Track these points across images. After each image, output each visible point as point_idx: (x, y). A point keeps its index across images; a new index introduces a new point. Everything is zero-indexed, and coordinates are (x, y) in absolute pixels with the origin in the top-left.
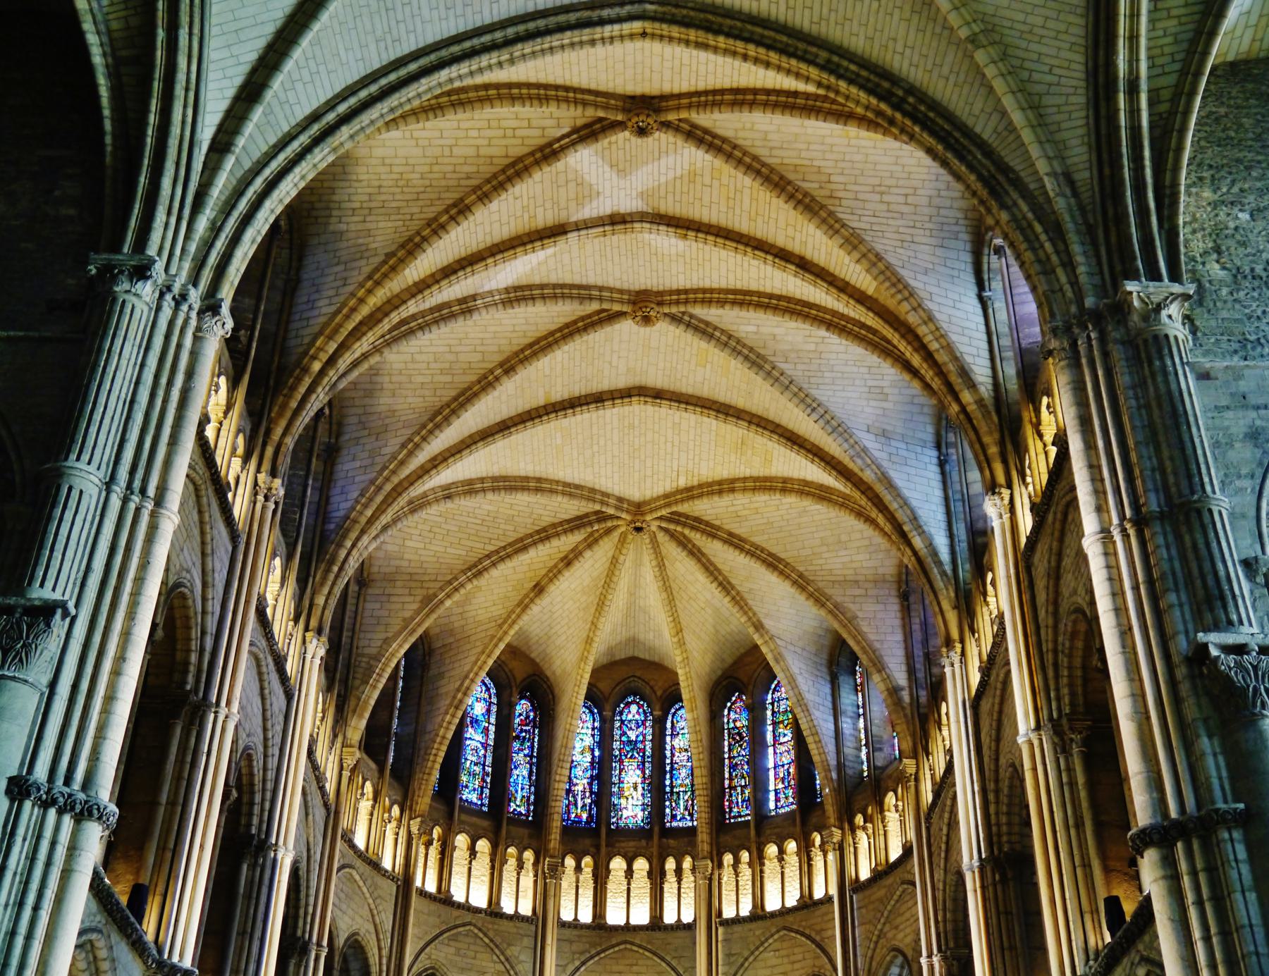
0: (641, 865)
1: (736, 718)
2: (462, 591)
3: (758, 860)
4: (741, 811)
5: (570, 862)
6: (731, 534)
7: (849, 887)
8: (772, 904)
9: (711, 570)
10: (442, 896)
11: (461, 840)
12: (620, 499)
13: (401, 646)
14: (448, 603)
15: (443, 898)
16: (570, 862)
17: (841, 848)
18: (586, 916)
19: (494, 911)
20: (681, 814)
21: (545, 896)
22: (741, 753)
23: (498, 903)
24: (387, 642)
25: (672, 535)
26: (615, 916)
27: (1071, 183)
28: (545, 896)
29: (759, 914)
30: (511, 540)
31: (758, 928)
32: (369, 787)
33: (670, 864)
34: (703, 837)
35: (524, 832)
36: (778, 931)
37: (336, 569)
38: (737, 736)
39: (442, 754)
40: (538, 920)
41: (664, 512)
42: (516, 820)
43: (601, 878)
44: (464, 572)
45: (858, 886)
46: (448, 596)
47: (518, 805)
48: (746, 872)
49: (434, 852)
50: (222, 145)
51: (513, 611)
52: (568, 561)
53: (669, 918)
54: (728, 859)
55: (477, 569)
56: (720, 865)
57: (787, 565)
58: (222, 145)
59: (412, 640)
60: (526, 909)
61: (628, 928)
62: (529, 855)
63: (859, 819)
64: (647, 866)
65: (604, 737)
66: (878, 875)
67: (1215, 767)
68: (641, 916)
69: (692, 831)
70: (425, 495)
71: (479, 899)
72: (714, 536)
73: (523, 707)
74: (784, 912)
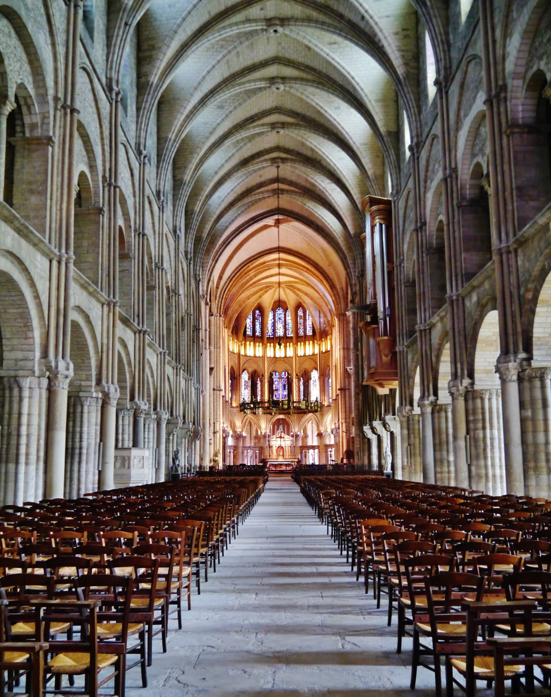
1: (300, 313)
3: (305, 344)
4: (301, 333)
5: (268, 344)
7: (321, 353)
8: (307, 354)
9: (294, 292)
15: (246, 356)
17: (320, 345)
19: (255, 356)
20: (290, 334)
21: (265, 352)
22: (302, 321)
24: (233, 314)
26: (277, 356)
27: (342, 289)
28: (265, 352)
29: (305, 356)
31: (304, 358)
33: (288, 344)
34: (294, 340)
35: (259, 340)
38: (300, 317)
40: (263, 357)
42: (258, 337)
43: (274, 347)
45: (322, 353)
47: (258, 334)
48: (302, 347)
49: (243, 346)
50: (217, 288)
52: (266, 292)
53: (288, 356)
55: (248, 298)
58: (217, 288)
60: (261, 355)
62: (261, 344)
65: (274, 318)
66: (326, 352)
67: (347, 383)
68: (283, 355)
69: (292, 337)
73: (257, 312)
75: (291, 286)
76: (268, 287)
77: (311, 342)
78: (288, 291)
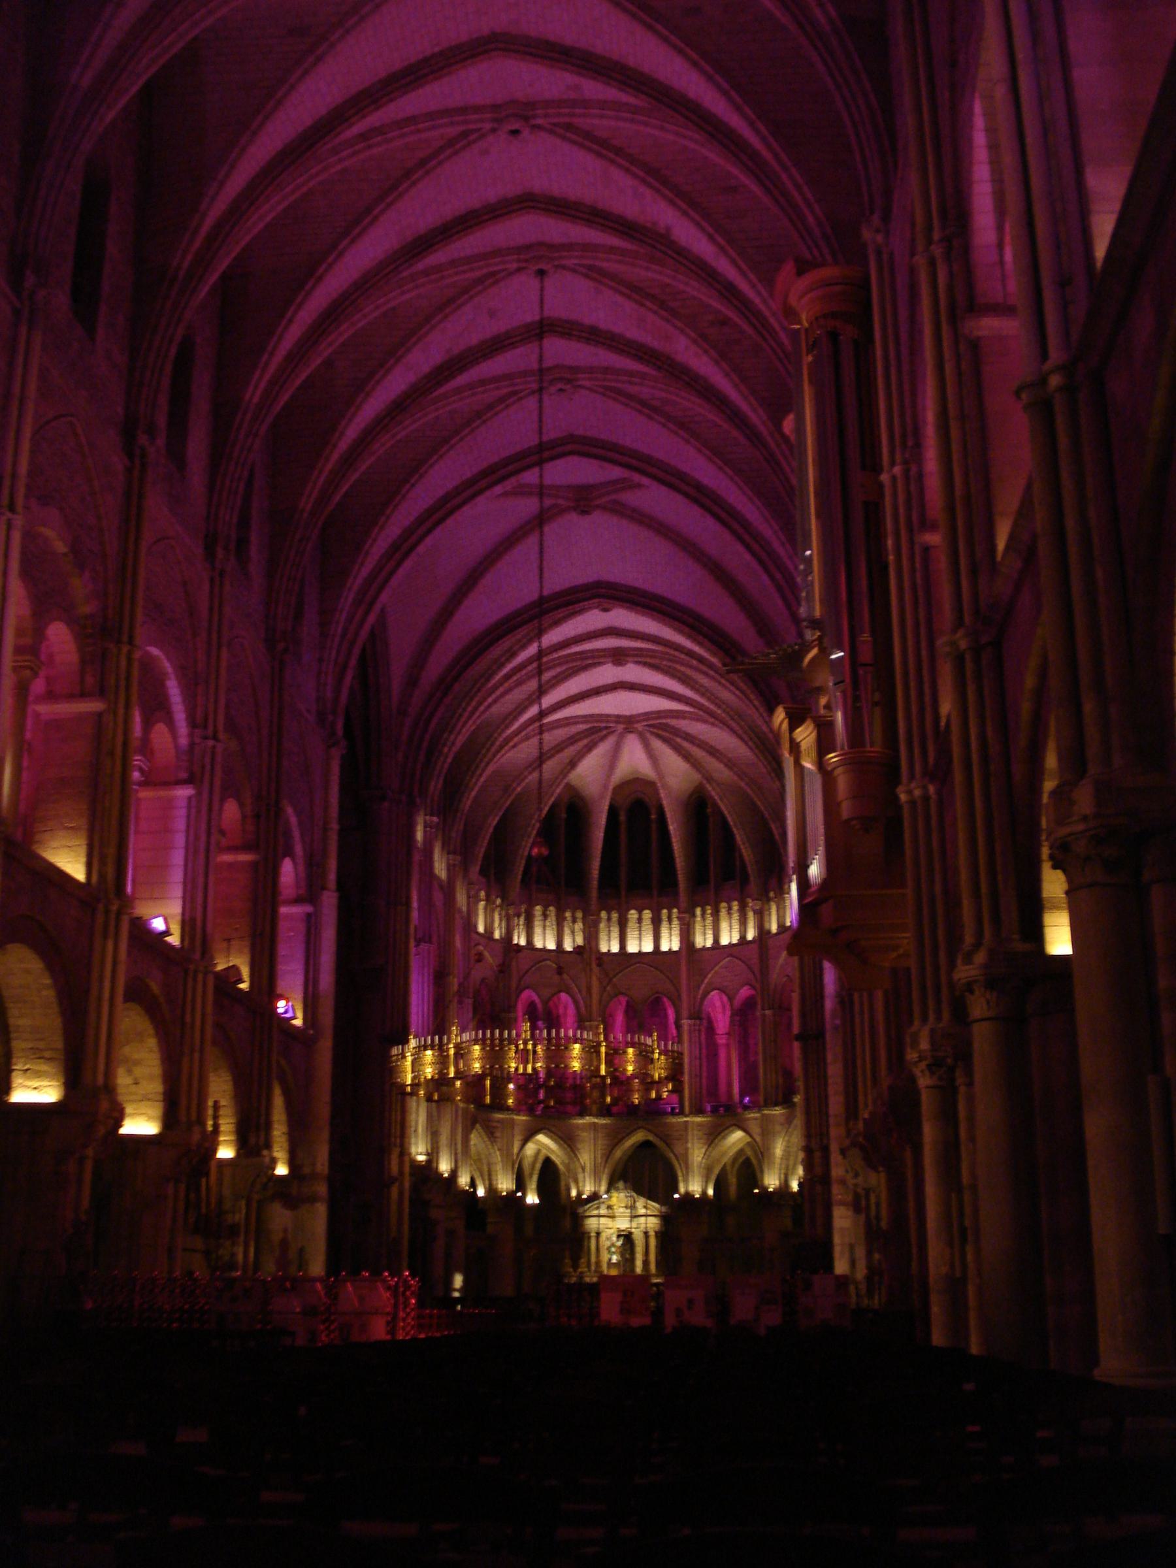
0: (647, 914)
2: (527, 781)
5: (604, 914)
6: (688, 734)
8: (724, 941)
10: (529, 947)
11: (538, 910)
12: (618, 716)
13: (494, 819)
14: (519, 789)
16: (604, 914)
18: (615, 948)
23: (562, 945)
25: (652, 733)
26: (632, 948)
30: (553, 745)
32: (482, 894)
36: (728, 957)
37: (459, 814)
39: (523, 865)
41: (646, 723)
44: (527, 768)
46: (519, 784)
48: (709, 920)
51: (557, 778)
52: (589, 748)
54: (698, 911)
56: (694, 915)
57: (721, 754)
59: (501, 813)
61: (640, 954)
62: (579, 915)
63: (772, 894)
64: (650, 916)
68: (648, 947)
70: (495, 684)
71: (551, 946)
72: (677, 735)
74: (730, 946)
75: (665, 727)
76: (592, 731)
77: (735, 906)
78: (657, 744)
